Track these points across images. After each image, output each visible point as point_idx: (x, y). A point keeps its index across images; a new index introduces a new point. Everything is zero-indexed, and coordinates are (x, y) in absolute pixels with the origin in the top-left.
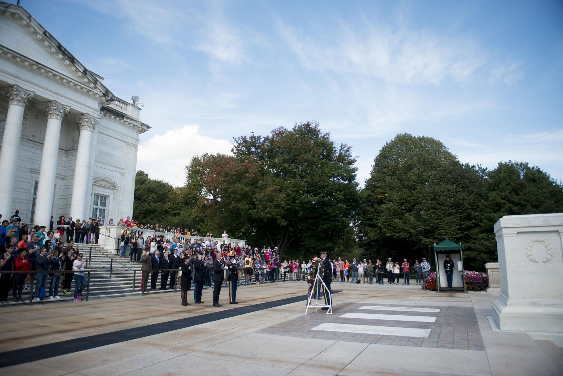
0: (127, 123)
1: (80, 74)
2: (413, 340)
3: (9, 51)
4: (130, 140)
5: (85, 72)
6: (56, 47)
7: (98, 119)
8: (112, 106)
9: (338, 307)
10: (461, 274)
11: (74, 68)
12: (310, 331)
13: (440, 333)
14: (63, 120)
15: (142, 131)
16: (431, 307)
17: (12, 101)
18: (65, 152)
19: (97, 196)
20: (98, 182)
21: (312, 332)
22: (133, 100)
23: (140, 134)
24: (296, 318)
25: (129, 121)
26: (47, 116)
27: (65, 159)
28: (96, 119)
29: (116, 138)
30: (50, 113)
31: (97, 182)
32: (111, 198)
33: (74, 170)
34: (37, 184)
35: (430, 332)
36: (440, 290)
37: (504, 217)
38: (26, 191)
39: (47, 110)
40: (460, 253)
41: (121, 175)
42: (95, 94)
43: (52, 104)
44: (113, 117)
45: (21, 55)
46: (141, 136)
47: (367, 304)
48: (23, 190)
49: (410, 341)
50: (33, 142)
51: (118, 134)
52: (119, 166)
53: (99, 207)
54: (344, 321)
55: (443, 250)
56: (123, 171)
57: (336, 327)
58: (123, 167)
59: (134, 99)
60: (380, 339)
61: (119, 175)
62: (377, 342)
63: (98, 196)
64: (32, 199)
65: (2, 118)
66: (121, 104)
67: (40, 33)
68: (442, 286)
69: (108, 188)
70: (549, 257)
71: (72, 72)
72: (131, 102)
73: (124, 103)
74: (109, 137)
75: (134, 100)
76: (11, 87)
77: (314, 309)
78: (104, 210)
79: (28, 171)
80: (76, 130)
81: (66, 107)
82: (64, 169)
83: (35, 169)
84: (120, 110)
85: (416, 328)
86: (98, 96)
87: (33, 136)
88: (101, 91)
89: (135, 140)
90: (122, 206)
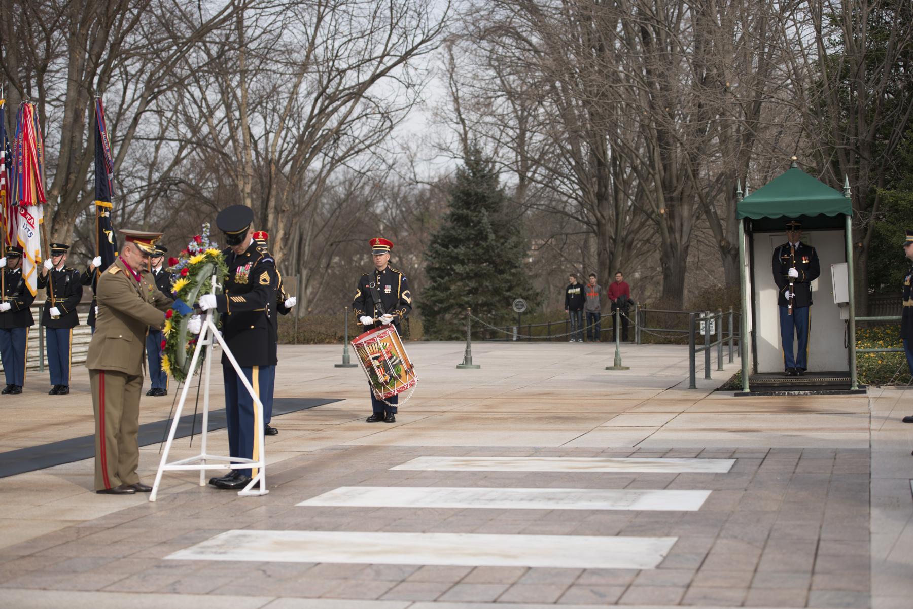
2: (595, 579)
9: (301, 464)
10: (844, 316)
12: (158, 567)
13: (711, 549)
16: (699, 455)
21: (171, 567)
24: (105, 518)
35: (672, 548)
36: (750, 388)
40: (843, 227)
47: (432, 448)
49: (579, 585)
54: (317, 519)
55: (775, 214)
57: (276, 543)
60: (457, 583)
62: (444, 593)
68: (761, 369)
77: (197, 474)
85: (618, 534)
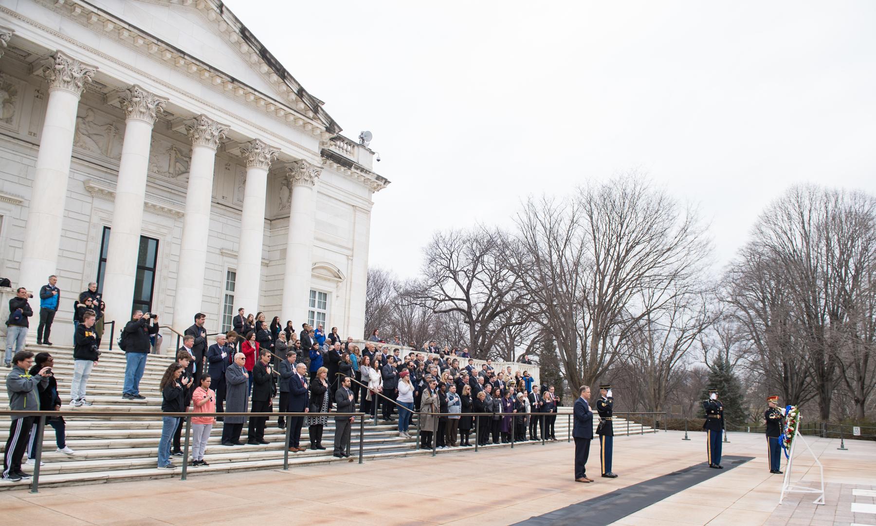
0: (356, 176)
1: (293, 97)
3: (194, 61)
5: (301, 92)
6: (258, 52)
7: (320, 169)
8: (333, 148)
11: (284, 87)
14: (270, 169)
15: (377, 188)
17: (198, 141)
18: (269, 222)
19: (313, 292)
20: (314, 271)
22: (362, 138)
23: (374, 192)
25: (358, 172)
26: (245, 166)
27: (268, 234)
28: (315, 168)
29: (340, 201)
30: (252, 159)
31: (318, 270)
32: (334, 295)
33: (284, 252)
34: (232, 275)
38: (216, 284)
39: (247, 155)
41: (348, 259)
42: (314, 128)
43: (253, 146)
44: (335, 165)
46: (376, 196)
48: (211, 282)
50: (224, 207)
51: (341, 193)
53: (316, 310)
56: (349, 253)
58: (350, 246)
59: (364, 137)
63: (315, 292)
64: (224, 296)
65: (179, 169)
67: (235, 32)
69: (329, 280)
71: (279, 94)
72: (357, 141)
73: (350, 143)
75: (365, 138)
76: (195, 118)
78: (325, 314)
79: (218, 251)
80: (285, 188)
81: (275, 150)
82: (267, 248)
83: (228, 250)
84: (344, 154)
86: (319, 132)
89: (367, 203)
90: (349, 308)
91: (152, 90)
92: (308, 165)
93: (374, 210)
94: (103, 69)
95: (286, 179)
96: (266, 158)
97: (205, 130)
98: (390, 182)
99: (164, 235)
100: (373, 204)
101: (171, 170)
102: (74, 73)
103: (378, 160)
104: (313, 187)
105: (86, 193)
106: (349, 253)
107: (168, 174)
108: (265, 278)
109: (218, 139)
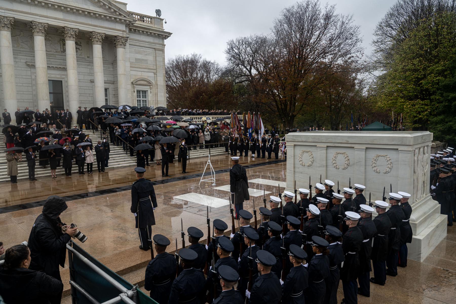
0: (153, 34)
4: (157, 47)
19: (138, 92)
27: (112, 69)
32: (149, 91)
37: (289, 134)
38: (91, 95)
41: (155, 74)
45: (63, 4)
46: (166, 41)
51: (148, 44)
52: (152, 68)
53: (141, 99)
56: (155, 71)
58: (155, 68)
59: (158, 12)
61: (152, 74)
66: (147, 19)
70: (310, 163)
74: (141, 47)
78: (146, 101)
79: (89, 81)
82: (113, 76)
87: (88, 57)
88: (125, 16)
89: (161, 46)
91: (41, 21)
92: (121, 38)
93: (166, 49)
94: (17, 17)
95: (115, 44)
96: (99, 39)
97: (68, 33)
98: (172, 33)
99: (63, 78)
100: (165, 45)
101: (62, 50)
102: (5, 23)
103: (166, 23)
104: (126, 47)
105: (27, 67)
106: (155, 71)
107: (61, 52)
108: (113, 89)
109: (75, 35)
